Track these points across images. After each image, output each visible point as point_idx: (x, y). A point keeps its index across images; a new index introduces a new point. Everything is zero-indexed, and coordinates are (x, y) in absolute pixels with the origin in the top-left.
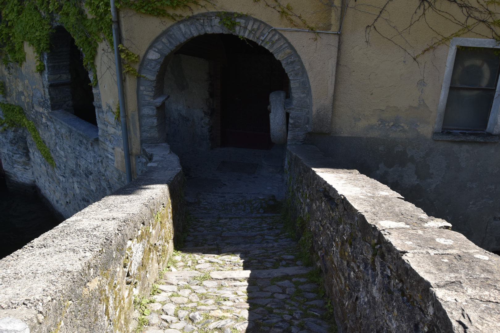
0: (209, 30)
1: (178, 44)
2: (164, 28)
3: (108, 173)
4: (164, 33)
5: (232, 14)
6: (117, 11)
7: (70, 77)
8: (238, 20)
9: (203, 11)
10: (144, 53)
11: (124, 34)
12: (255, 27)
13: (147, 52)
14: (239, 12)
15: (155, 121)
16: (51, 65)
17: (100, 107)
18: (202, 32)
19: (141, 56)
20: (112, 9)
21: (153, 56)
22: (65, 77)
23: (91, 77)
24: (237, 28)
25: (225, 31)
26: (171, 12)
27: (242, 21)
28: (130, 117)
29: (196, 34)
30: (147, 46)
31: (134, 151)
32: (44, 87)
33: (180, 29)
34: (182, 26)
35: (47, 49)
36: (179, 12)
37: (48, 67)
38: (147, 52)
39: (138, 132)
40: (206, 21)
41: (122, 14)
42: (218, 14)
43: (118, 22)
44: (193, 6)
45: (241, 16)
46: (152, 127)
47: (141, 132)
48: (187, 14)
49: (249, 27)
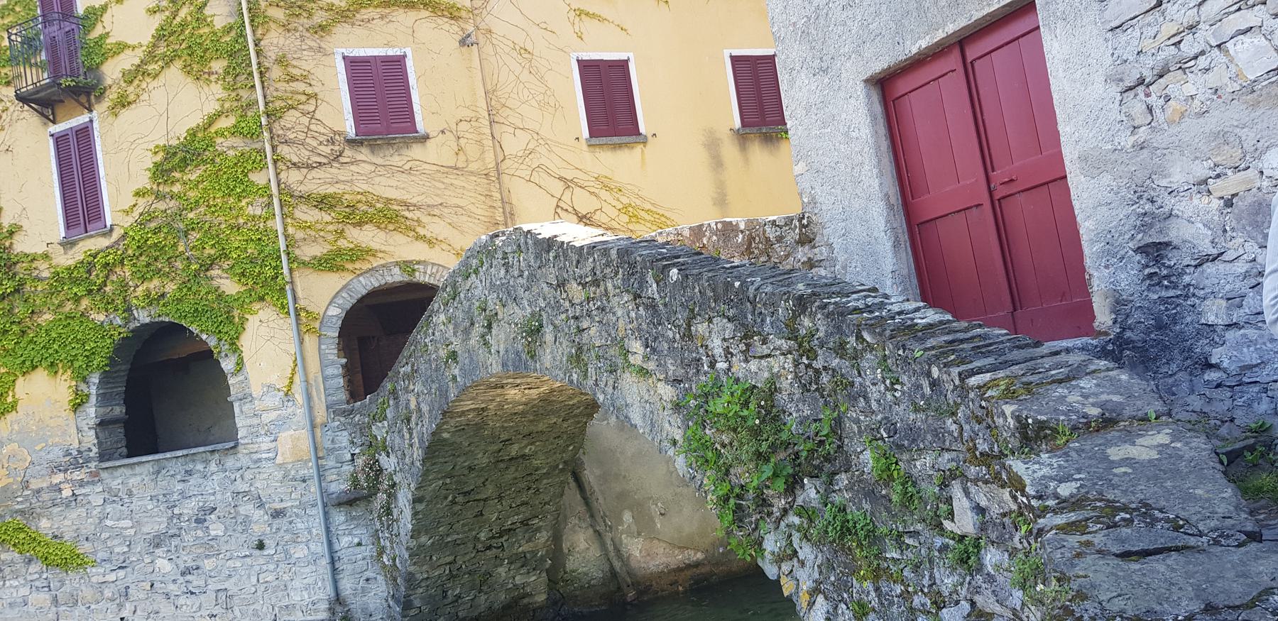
0: (390, 279)
1: (360, 296)
2: (344, 283)
3: (258, 484)
4: (344, 287)
5: (411, 262)
6: (291, 270)
7: (124, 411)
8: (416, 267)
9: (382, 262)
10: (324, 309)
11: (300, 294)
12: (434, 270)
13: (327, 308)
14: (417, 259)
15: (342, 380)
16: (101, 391)
17: (246, 397)
18: (383, 282)
19: (321, 314)
20: (285, 271)
21: (334, 311)
22: (119, 410)
23: (227, 365)
24: (417, 274)
25: (406, 278)
26: (349, 266)
27: (421, 267)
28: (312, 382)
29: (377, 285)
30: (329, 301)
31: (319, 420)
32: (79, 430)
33: (360, 282)
34: (361, 278)
35: (106, 365)
36: (357, 265)
37: (98, 395)
38: (327, 308)
39: (323, 396)
40: (385, 271)
41: (296, 274)
42: (397, 263)
43: (292, 282)
44: (371, 259)
45: (418, 263)
46: (338, 389)
47: (327, 396)
48: (366, 266)
49: (429, 272)
